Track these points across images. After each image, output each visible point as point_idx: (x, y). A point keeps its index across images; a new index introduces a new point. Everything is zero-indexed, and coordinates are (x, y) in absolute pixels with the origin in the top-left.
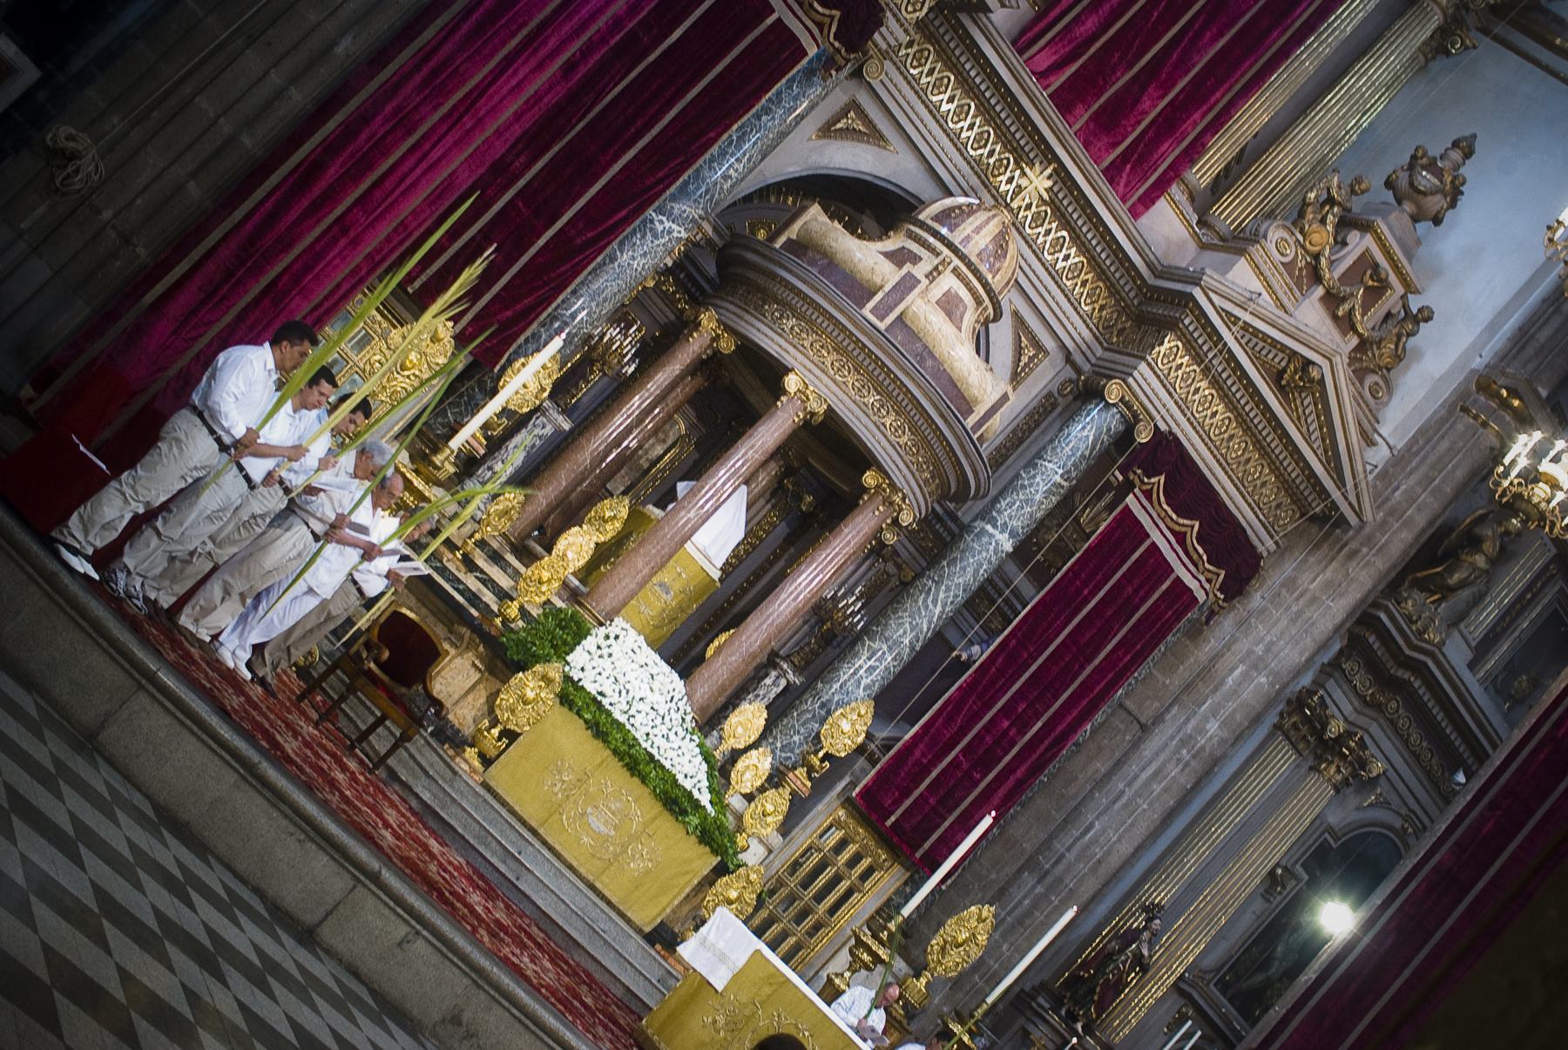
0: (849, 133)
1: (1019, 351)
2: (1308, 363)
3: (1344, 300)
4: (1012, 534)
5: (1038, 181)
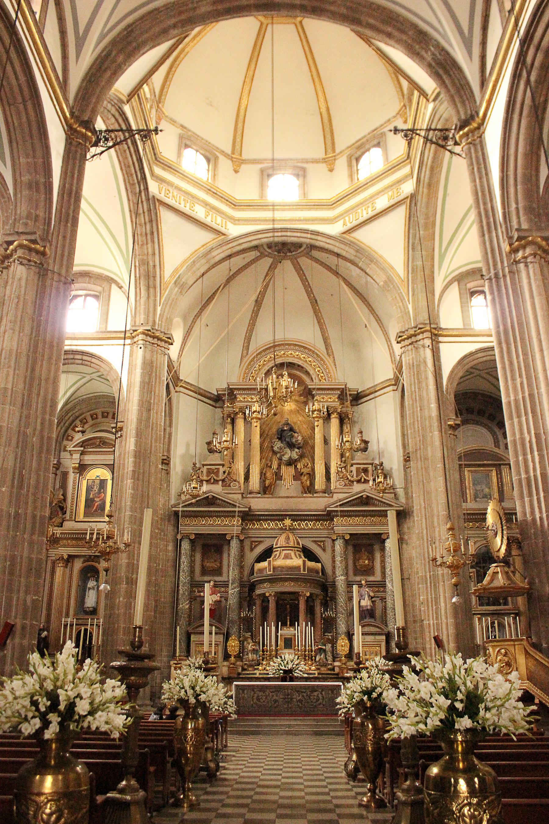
0: (256, 546)
1: (320, 546)
2: (362, 496)
3: (361, 479)
4: (342, 575)
5: (288, 522)
